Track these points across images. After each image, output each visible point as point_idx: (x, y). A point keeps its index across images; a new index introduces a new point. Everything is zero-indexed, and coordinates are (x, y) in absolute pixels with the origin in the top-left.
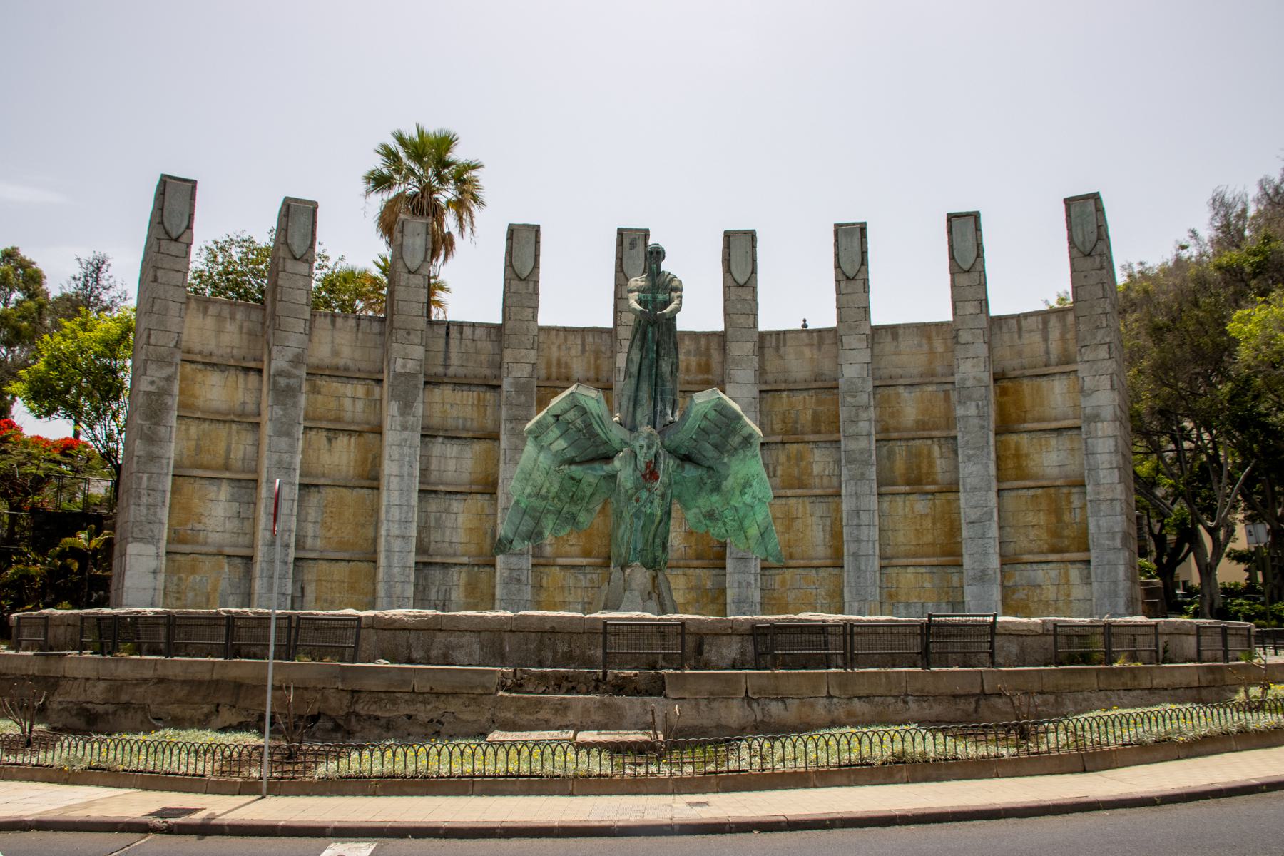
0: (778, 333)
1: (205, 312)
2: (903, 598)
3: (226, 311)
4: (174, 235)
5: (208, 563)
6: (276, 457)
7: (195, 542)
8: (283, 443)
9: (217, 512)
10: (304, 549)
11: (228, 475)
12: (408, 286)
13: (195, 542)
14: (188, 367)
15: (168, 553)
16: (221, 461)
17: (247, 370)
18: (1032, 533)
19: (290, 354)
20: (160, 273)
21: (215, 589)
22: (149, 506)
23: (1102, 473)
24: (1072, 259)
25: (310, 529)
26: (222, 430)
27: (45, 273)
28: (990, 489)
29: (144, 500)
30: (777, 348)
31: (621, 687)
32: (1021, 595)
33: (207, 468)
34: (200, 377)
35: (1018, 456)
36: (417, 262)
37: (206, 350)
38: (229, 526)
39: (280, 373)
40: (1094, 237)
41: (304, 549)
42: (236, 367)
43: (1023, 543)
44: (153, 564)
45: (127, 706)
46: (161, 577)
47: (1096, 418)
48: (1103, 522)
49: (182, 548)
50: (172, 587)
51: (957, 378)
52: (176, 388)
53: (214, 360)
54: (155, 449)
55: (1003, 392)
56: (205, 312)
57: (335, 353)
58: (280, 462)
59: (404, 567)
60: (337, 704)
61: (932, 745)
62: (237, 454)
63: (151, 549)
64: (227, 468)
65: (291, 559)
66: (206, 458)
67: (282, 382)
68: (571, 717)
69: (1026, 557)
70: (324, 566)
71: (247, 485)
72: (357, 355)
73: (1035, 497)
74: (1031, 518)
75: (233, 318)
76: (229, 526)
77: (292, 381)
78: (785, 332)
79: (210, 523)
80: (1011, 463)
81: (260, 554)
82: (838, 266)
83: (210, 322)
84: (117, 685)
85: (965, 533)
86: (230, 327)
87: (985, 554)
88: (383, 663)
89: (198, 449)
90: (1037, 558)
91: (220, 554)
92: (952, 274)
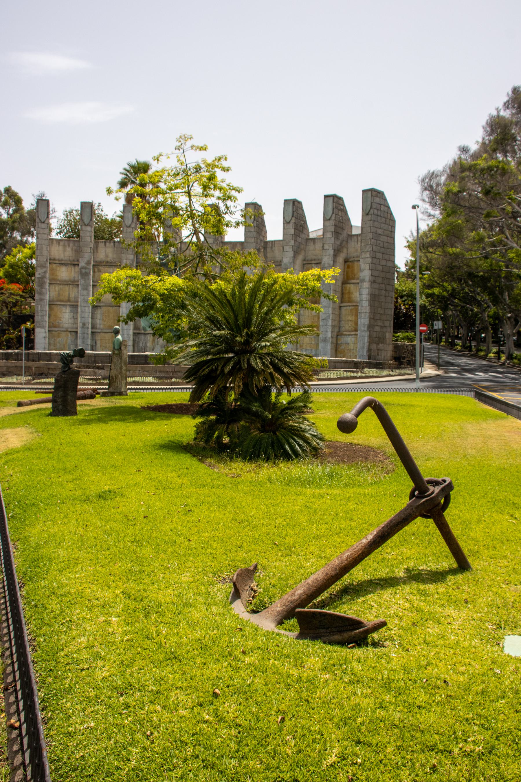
0: (272, 241)
1: (59, 244)
2: (304, 347)
3: (66, 243)
4: (43, 221)
5: (63, 334)
6: (82, 298)
7: (59, 327)
8: (85, 292)
9: (65, 316)
10: (96, 329)
11: (69, 303)
12: (127, 232)
13: (59, 327)
14: (54, 265)
15: (49, 331)
16: (67, 298)
17: (74, 265)
18: (350, 323)
19: (86, 260)
20: (39, 235)
21: (66, 343)
22: (41, 316)
23: (364, 302)
24: (362, 216)
25: (98, 322)
26: (67, 288)
27: (23, 198)
28: (329, 307)
29: (40, 314)
30: (272, 248)
31: (99, 368)
32: (343, 347)
33: (63, 301)
34: (58, 268)
35: (349, 293)
36: (130, 223)
37: (60, 258)
38: (70, 321)
39: (83, 268)
40: (369, 207)
41: (96, 329)
42: (71, 264)
43: (347, 327)
44: (44, 335)
45: (10, 372)
46: (47, 339)
47: (363, 281)
48: (362, 321)
49: (54, 329)
50: (52, 342)
51: (323, 263)
52: (48, 275)
53: (63, 262)
54: (42, 297)
55: (348, 267)
56: (59, 244)
57: (107, 256)
58: (84, 299)
59: (128, 335)
60: (46, 371)
61: (150, 379)
62: (72, 295)
63: (43, 330)
64: (69, 301)
65: (90, 332)
66: (62, 298)
67: (84, 271)
68: (87, 374)
69: (345, 333)
70: (103, 334)
71: (75, 307)
72: (115, 256)
73: (352, 309)
74: (350, 318)
75: (69, 246)
76: (70, 321)
77: (87, 271)
78: (275, 241)
79: (64, 320)
80: (347, 296)
81: (79, 330)
82: (284, 218)
83: (61, 248)
84: (8, 367)
85: (321, 324)
86: (69, 249)
87: (327, 331)
88: (55, 362)
89: (59, 295)
90: (348, 333)
91: (67, 331)
92: (324, 221)
